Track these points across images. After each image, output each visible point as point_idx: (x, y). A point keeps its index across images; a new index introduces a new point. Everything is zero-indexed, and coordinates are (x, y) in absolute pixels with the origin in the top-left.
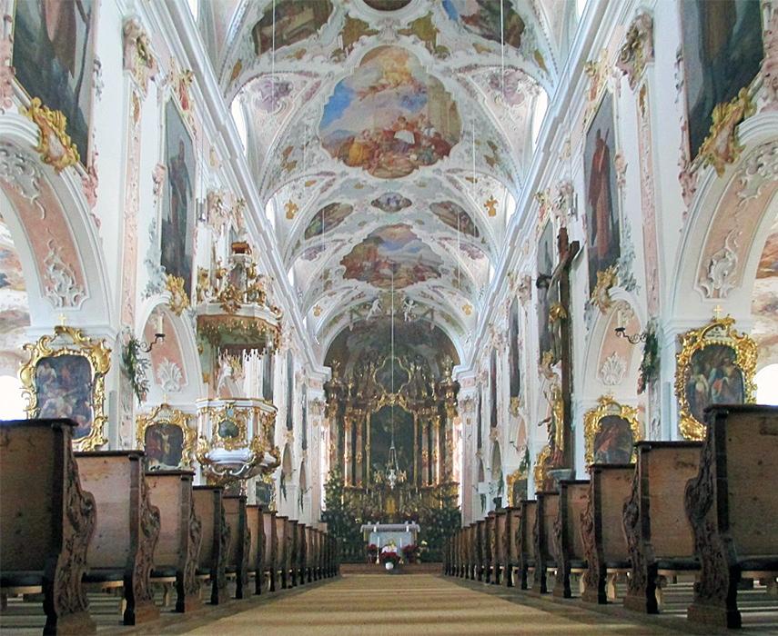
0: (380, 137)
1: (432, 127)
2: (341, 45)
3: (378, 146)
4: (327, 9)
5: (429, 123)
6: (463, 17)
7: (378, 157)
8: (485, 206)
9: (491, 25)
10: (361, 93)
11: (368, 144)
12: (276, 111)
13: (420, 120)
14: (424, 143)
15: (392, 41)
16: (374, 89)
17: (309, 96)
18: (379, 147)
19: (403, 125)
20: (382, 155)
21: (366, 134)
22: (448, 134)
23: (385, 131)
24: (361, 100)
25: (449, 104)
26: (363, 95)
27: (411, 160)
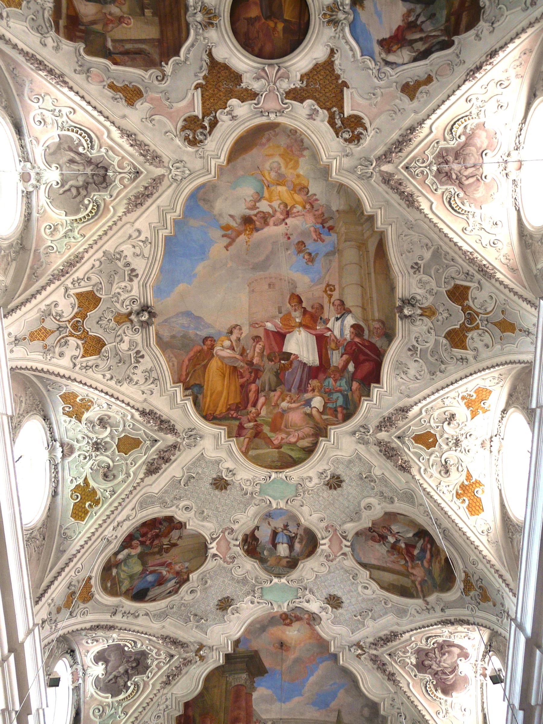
0: (259, 347)
1: (349, 312)
2: (198, 112)
3: (257, 372)
5: (342, 303)
6: (382, 43)
7: (254, 405)
9: (428, 27)
12: (80, 216)
13: (326, 299)
16: (247, 221)
21: (234, 337)
22: (377, 325)
23: (267, 331)
24: (227, 247)
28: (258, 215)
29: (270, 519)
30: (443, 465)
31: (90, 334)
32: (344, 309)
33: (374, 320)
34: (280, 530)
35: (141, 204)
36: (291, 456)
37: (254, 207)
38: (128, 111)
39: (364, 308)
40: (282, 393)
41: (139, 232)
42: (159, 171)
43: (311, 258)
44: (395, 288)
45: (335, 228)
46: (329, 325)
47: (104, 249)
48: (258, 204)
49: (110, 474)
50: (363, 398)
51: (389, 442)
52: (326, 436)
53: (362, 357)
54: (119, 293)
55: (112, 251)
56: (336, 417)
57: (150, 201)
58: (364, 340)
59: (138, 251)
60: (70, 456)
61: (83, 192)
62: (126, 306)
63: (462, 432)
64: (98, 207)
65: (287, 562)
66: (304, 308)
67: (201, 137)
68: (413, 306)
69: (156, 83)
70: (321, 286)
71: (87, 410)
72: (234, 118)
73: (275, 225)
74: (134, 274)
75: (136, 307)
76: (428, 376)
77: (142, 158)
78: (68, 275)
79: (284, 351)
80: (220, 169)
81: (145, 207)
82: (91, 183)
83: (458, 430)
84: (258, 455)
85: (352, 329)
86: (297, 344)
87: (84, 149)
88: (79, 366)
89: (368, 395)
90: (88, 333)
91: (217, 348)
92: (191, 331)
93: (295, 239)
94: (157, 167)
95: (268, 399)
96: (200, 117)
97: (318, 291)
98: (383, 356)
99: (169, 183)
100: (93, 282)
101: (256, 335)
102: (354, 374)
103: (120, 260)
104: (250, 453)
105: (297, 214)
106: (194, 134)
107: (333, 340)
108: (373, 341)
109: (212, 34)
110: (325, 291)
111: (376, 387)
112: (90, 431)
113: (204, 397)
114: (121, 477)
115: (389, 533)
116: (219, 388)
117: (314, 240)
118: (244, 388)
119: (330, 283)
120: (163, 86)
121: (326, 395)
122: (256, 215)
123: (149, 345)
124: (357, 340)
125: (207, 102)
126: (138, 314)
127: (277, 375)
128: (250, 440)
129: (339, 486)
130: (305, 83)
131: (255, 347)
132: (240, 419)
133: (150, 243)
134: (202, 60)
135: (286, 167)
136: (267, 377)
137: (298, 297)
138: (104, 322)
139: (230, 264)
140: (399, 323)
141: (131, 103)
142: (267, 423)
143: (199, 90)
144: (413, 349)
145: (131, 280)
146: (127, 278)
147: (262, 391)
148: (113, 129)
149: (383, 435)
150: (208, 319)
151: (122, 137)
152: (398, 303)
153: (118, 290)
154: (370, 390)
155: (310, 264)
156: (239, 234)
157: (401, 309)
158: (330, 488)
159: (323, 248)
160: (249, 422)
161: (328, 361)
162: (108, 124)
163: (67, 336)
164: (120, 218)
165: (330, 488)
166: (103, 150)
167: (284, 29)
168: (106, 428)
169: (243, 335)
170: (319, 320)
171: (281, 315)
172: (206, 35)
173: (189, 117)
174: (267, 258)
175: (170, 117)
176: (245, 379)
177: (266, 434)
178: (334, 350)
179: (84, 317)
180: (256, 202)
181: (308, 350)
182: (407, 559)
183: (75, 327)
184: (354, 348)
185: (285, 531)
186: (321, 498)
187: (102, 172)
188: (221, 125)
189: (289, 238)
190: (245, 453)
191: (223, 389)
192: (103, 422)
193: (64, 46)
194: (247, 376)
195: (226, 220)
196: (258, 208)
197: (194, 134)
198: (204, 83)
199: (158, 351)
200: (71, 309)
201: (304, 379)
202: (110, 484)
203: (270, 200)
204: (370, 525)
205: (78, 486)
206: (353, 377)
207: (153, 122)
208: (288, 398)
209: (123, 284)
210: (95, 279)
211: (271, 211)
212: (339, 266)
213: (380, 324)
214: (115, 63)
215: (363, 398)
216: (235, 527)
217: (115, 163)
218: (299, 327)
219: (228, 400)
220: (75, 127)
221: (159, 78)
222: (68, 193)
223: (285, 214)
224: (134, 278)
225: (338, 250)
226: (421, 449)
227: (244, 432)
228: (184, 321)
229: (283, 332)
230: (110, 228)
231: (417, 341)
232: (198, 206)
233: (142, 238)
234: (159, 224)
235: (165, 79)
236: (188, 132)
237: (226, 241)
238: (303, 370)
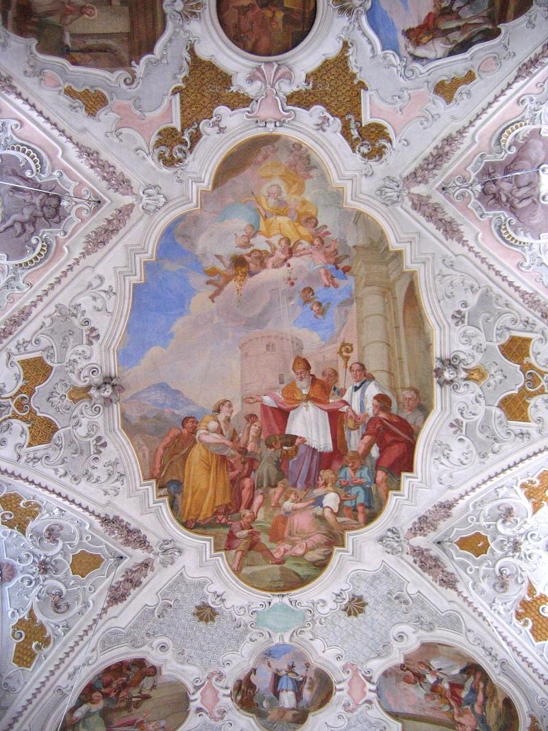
0: (254, 429)
2: (177, 124)
3: (251, 462)
4: (154, 22)
5: (363, 367)
7: (249, 506)
8: (519, 616)
10: (213, 272)
11: (230, 452)
12: (26, 259)
13: (341, 363)
14: (355, 441)
15: (281, 123)
16: (239, 262)
17: (100, 238)
18: (252, 469)
19: (304, 388)
20: (258, 500)
21: (221, 417)
23: (264, 407)
24: (212, 298)
25: (400, 292)
26: (218, 282)
27: (327, 513)
28: (253, 255)
29: (270, 659)
30: (497, 577)
31: (39, 414)
32: (365, 376)
33: (403, 388)
34: (283, 672)
35: (104, 243)
36: (296, 574)
37: (248, 245)
38: (88, 122)
39: (390, 373)
40: (284, 489)
41: (101, 279)
42: (128, 200)
43: (322, 309)
44: (431, 345)
45: (351, 270)
46: (346, 398)
47: (57, 301)
48: (252, 241)
49: (62, 603)
50: (391, 493)
51: (427, 550)
52: (343, 546)
53: (389, 439)
54: (75, 361)
55: (67, 305)
56: (357, 520)
57: (115, 238)
58: (391, 415)
59: (99, 304)
60: (10, 580)
61: (30, 229)
62: (84, 377)
63: (522, 531)
64: (49, 247)
65: (294, 715)
66: (312, 375)
67: (180, 155)
68: (455, 367)
69: (124, 86)
70: (335, 345)
71: (34, 517)
72: (221, 130)
73: (274, 267)
74: (94, 334)
75: (97, 379)
76: (478, 459)
77: (105, 183)
78: (11, 337)
79: (287, 432)
80: (204, 195)
81: (108, 246)
82: (40, 217)
83: (515, 529)
84: (254, 574)
85: (376, 402)
86: (305, 424)
87: (32, 172)
88: (25, 458)
89: (398, 489)
90: (35, 414)
91: (201, 432)
92: (166, 410)
93: (300, 285)
94: (124, 194)
95: (266, 499)
96: (179, 129)
97: (331, 352)
98: (417, 435)
99: (140, 215)
100: (43, 346)
101: (250, 412)
102: (378, 461)
103: (76, 316)
104: (244, 571)
105: (302, 252)
106: (171, 151)
107: (351, 417)
108: (403, 416)
109: (195, 27)
110: (340, 352)
111: (407, 477)
112: (36, 547)
113: (183, 497)
114: (77, 608)
115: (427, 670)
116: (203, 485)
117: (325, 286)
118: (235, 483)
119: (346, 341)
120: (133, 91)
121: (343, 490)
122: (249, 255)
123: (113, 430)
124: (382, 415)
125: (188, 111)
126: (99, 388)
127: (278, 465)
128: (244, 555)
129: (361, 611)
130: (311, 85)
131: (249, 429)
132: (230, 526)
133: (115, 294)
134: (181, 56)
135: (288, 193)
136: (265, 468)
137: (305, 361)
138: (56, 399)
139: (216, 320)
140: (437, 389)
141: (92, 112)
142: (266, 531)
143: (178, 96)
144: (456, 425)
145: (90, 343)
146: (85, 341)
147: (258, 487)
148: (70, 145)
149: (419, 541)
150: (189, 392)
151: (80, 157)
152: (436, 365)
153: (74, 357)
154: (400, 481)
155: (320, 316)
156: (228, 279)
157: (439, 372)
158: (349, 614)
159: (337, 295)
160: (243, 529)
161: (344, 445)
162: (63, 139)
163: (10, 418)
164: (77, 261)
165: (349, 614)
166: (56, 173)
167: (285, 19)
168: (57, 542)
169: (234, 414)
170: (332, 392)
171: (283, 386)
172: (187, 27)
173: (165, 130)
174: (265, 312)
175: (142, 132)
176: (237, 472)
177: (265, 545)
178: (352, 430)
179: (31, 392)
180: (249, 237)
181: (318, 431)
182: (452, 703)
183: (20, 406)
184: (378, 426)
185: (290, 674)
186: (337, 628)
187: (54, 202)
188: (206, 140)
189: (292, 284)
190: (237, 572)
191: (209, 484)
192: (52, 534)
193: (13, 43)
194: (239, 467)
195: (210, 263)
196: (253, 245)
197: (171, 151)
198: (184, 86)
199: (123, 437)
200: (15, 382)
201: (314, 471)
202: (62, 618)
203: (268, 236)
204: (402, 661)
205: (21, 621)
206: (378, 465)
207: (120, 137)
208: (292, 496)
209: (80, 349)
210: (45, 341)
211: (269, 250)
212: (358, 319)
213: (412, 393)
214: (74, 63)
215: (391, 493)
216: (226, 670)
217: (71, 191)
218: (306, 401)
219: (215, 500)
220: (22, 145)
221: (128, 81)
222: (11, 230)
223: (287, 252)
224: (94, 341)
225: (356, 298)
226: (467, 557)
227: (236, 543)
228: (157, 396)
229: (285, 408)
230: (65, 274)
231: (462, 413)
232: (176, 243)
233: (105, 287)
234: (125, 269)
235: (135, 84)
236: (163, 148)
237: (212, 289)
238: (312, 458)
